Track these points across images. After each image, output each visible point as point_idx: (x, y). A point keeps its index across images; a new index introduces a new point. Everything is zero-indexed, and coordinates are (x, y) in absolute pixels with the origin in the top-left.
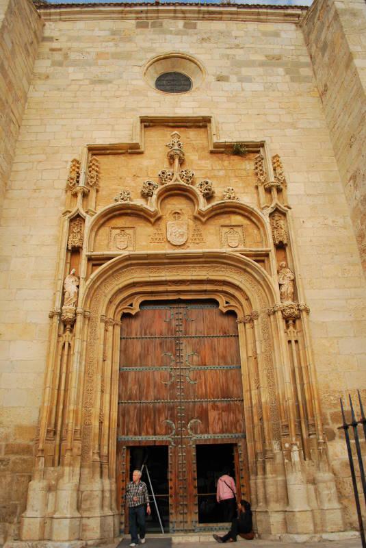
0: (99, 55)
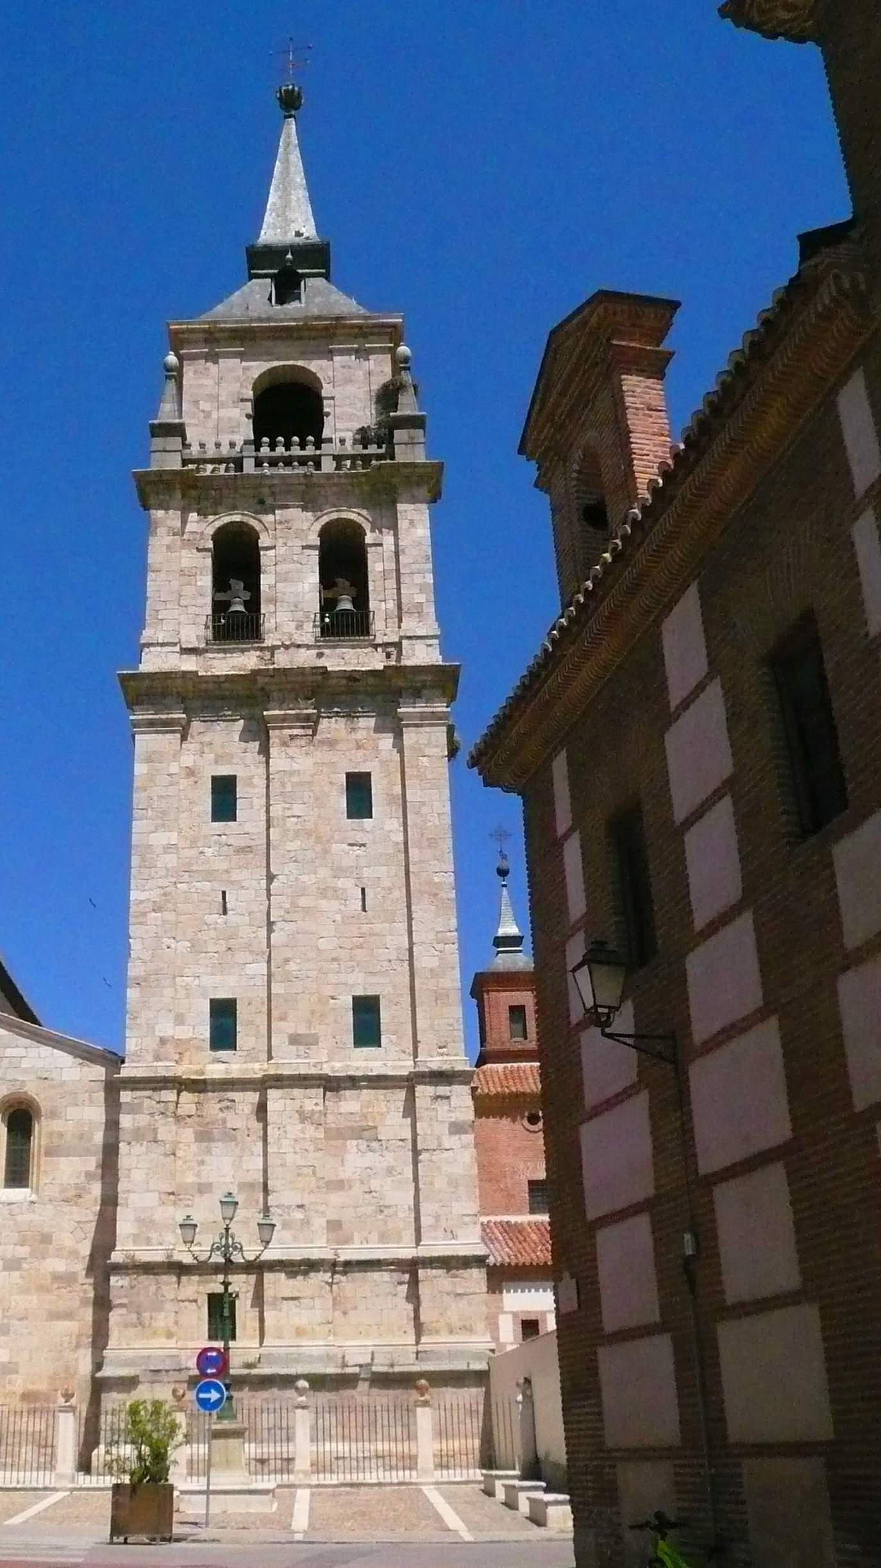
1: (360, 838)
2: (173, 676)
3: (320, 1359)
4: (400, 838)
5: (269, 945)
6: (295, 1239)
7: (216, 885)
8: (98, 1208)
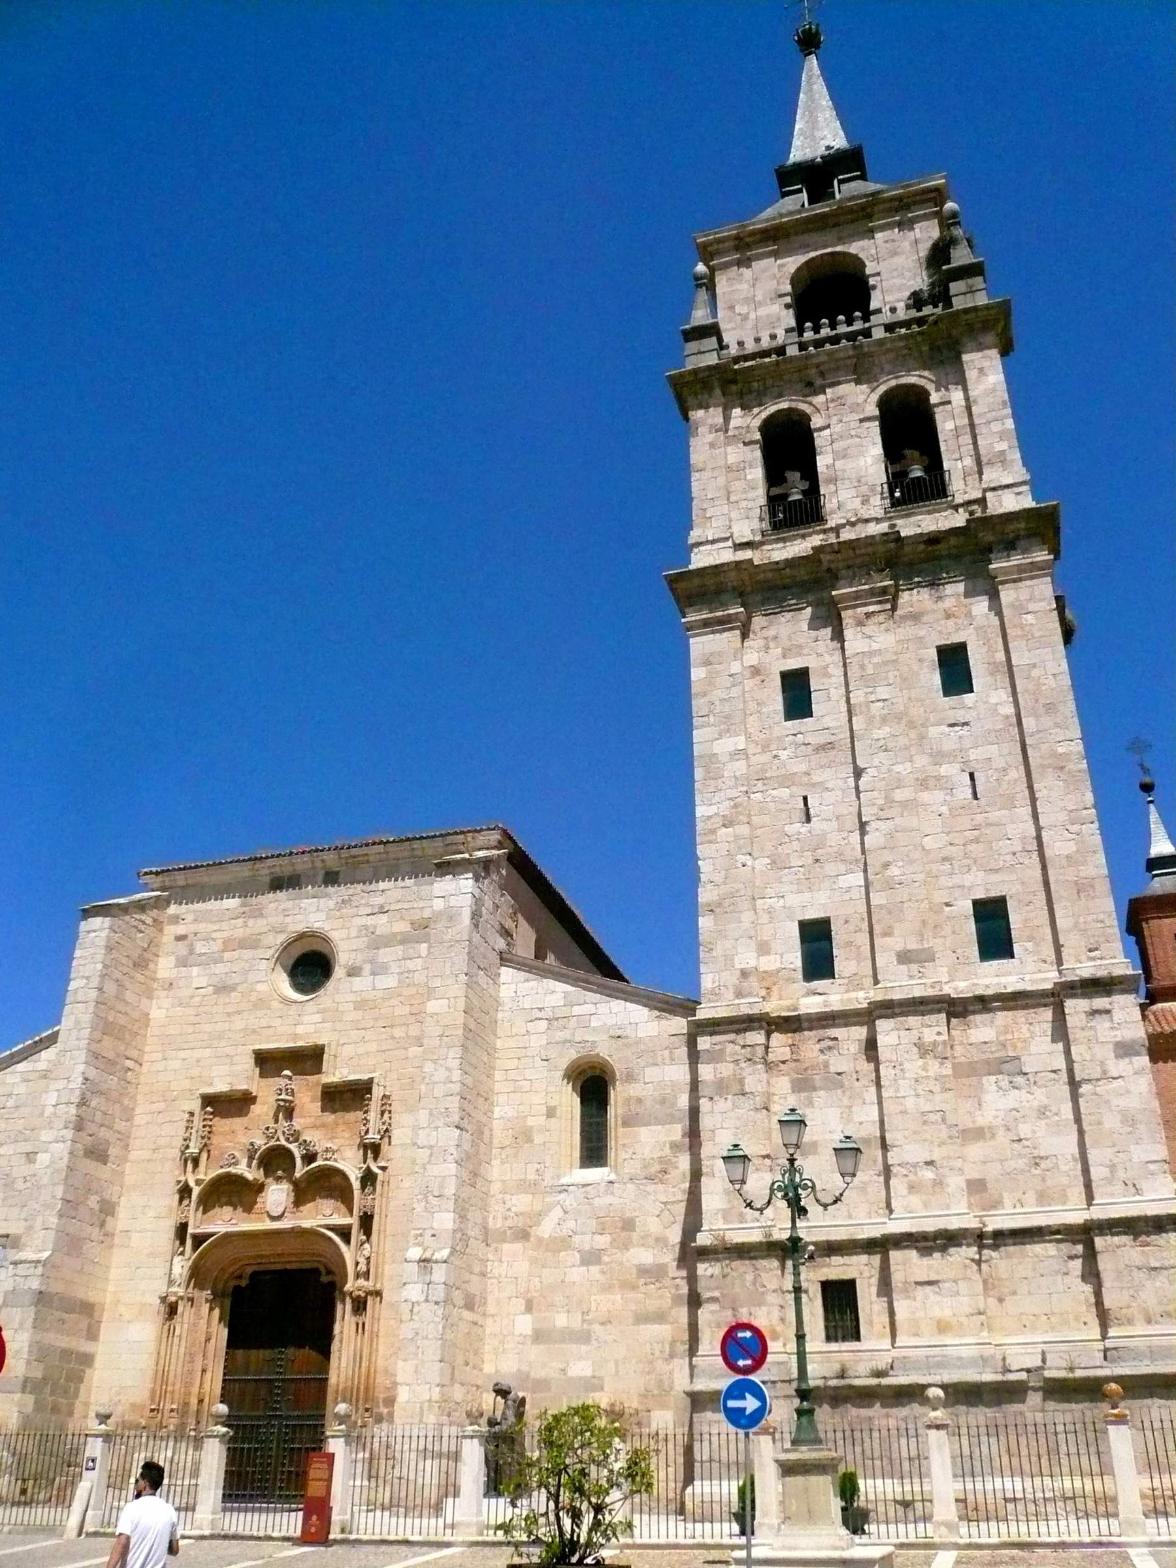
0: (228, 945)
1: (961, 716)
3: (971, 1362)
4: (1010, 710)
5: (863, 852)
6: (925, 1206)
7: (794, 789)
8: (688, 1185)
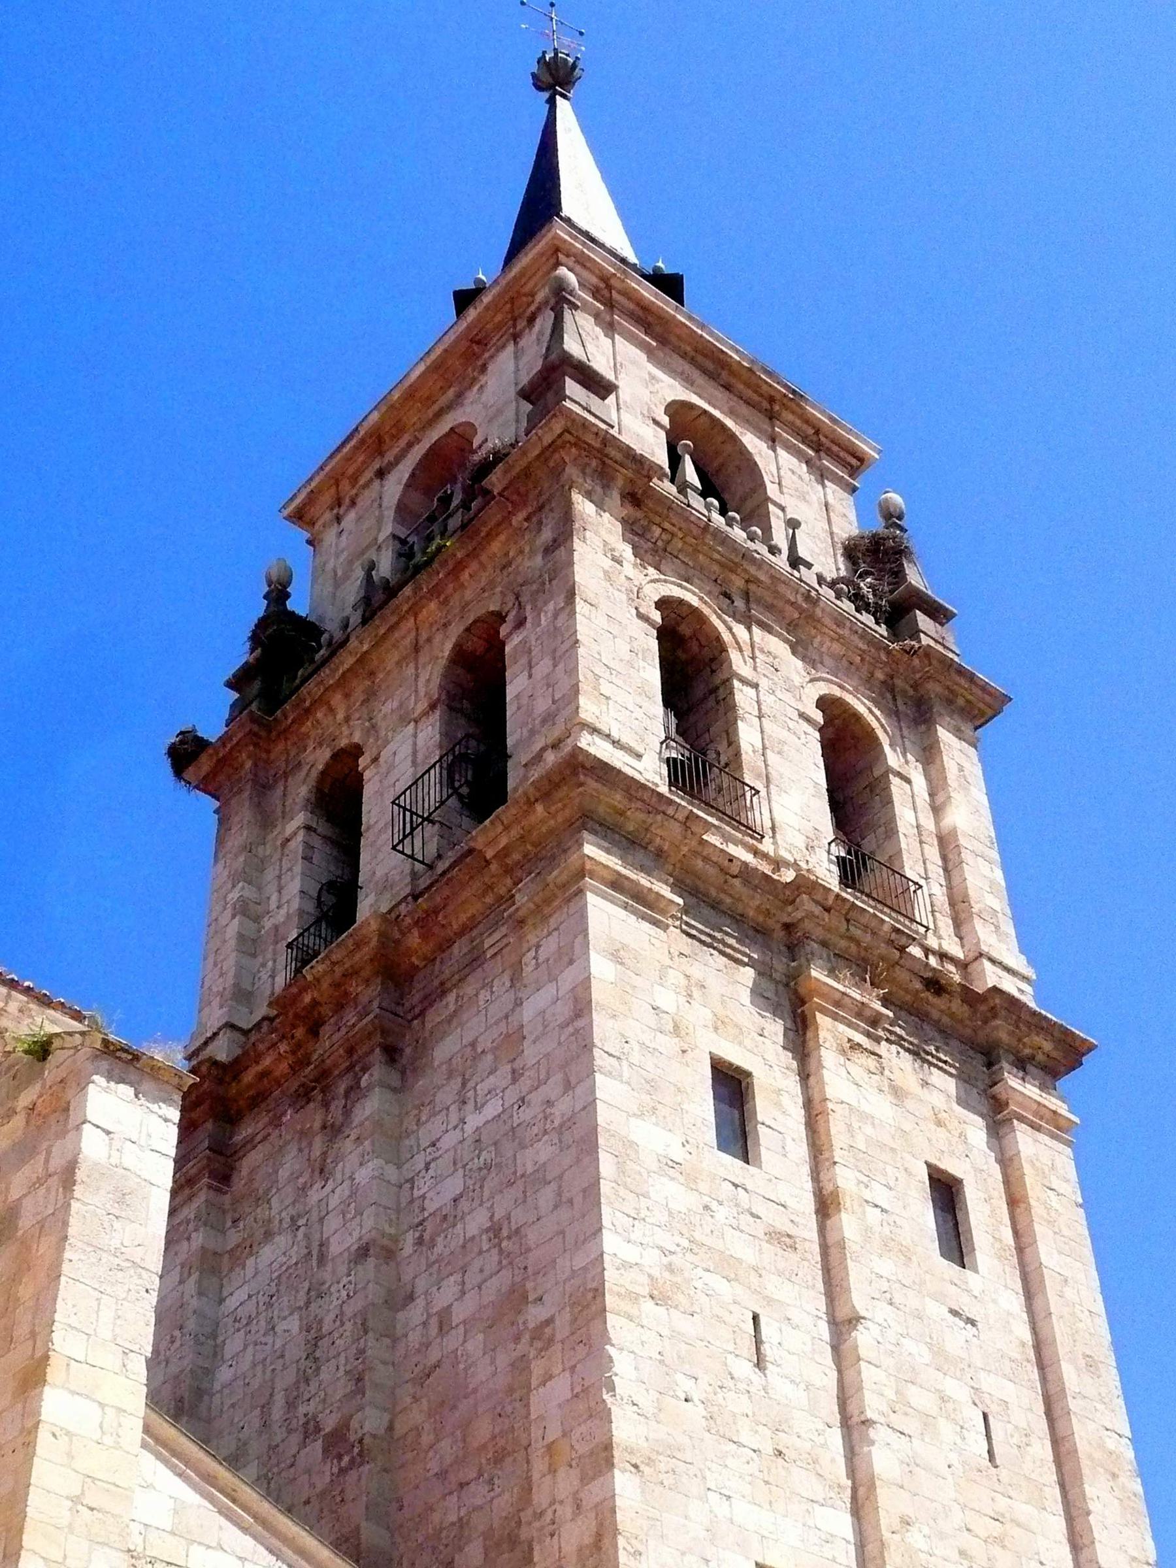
2: (670, 811)
